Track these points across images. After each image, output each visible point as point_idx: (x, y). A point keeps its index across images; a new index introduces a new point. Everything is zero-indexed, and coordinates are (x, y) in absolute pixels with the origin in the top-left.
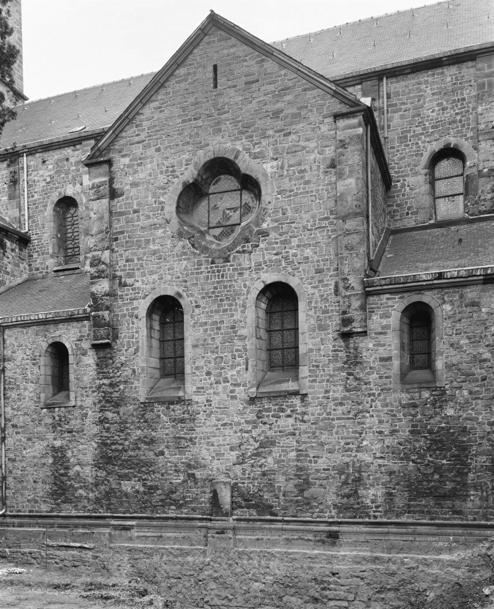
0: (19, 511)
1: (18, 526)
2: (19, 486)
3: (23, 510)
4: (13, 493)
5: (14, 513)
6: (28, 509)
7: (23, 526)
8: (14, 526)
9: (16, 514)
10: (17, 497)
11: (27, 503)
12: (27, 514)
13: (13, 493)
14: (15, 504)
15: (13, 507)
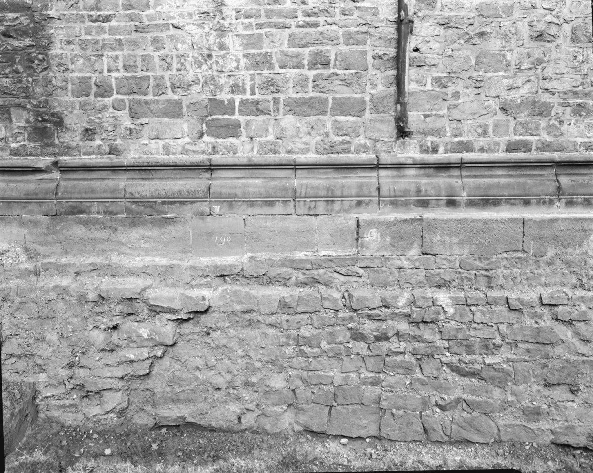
0: (466, 147)
1: (471, 204)
2: (468, 53)
3: (482, 141)
4: (437, 81)
5: (441, 156)
6: (503, 140)
7: (496, 203)
8: (451, 204)
9: (454, 157)
10: (456, 95)
11: (500, 116)
12: (501, 155)
13: (437, 81)
14: (445, 122)
15: (439, 132)
